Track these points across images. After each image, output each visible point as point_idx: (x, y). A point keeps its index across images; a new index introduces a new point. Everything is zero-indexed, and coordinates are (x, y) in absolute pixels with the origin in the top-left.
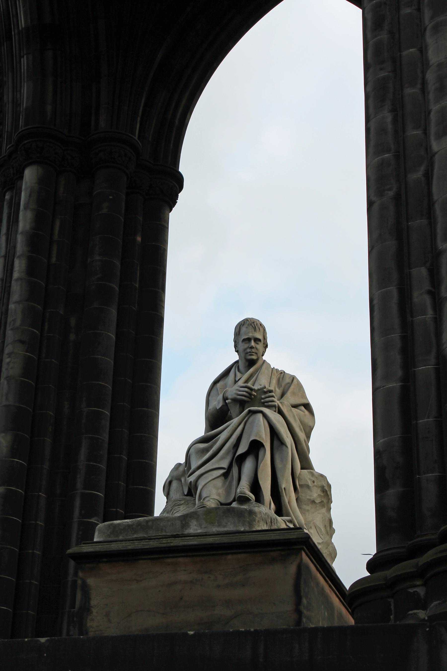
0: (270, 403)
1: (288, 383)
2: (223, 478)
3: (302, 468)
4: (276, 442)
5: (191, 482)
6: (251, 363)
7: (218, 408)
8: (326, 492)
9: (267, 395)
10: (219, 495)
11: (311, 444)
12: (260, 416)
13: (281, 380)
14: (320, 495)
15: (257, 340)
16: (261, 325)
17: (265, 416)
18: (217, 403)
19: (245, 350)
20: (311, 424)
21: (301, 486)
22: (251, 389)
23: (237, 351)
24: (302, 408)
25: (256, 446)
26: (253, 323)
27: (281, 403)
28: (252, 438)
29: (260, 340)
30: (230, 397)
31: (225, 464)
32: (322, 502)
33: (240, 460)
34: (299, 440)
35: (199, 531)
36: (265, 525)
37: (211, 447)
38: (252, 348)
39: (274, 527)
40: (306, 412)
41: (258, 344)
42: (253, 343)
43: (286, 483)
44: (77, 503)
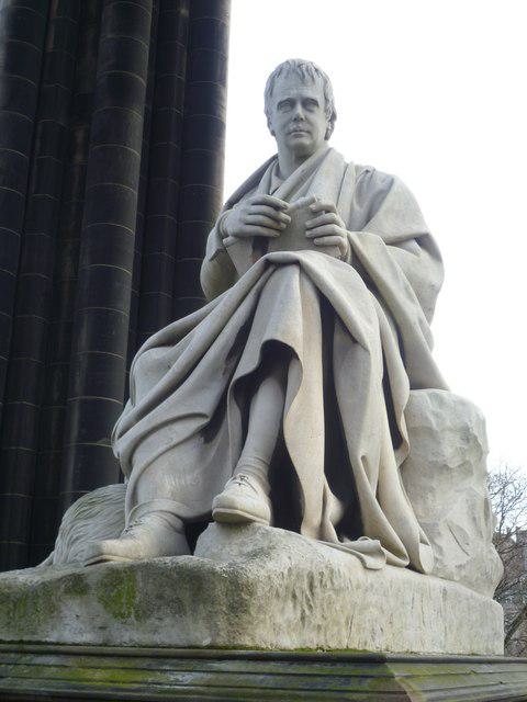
0: (326, 239)
3: (414, 386)
4: (338, 338)
9: (318, 219)
11: (436, 327)
12: (294, 275)
13: (365, 185)
15: (309, 103)
16: (316, 70)
19: (285, 126)
20: (434, 280)
22: (277, 208)
24: (414, 244)
25: (278, 358)
26: (299, 66)
27: (360, 236)
28: (267, 337)
29: (315, 102)
30: (230, 230)
31: (205, 403)
33: (245, 391)
34: (407, 321)
35: (87, 637)
37: (175, 358)
38: (297, 120)
40: (424, 255)
41: (311, 111)
42: (299, 110)
43: (371, 443)
44: (76, 417)
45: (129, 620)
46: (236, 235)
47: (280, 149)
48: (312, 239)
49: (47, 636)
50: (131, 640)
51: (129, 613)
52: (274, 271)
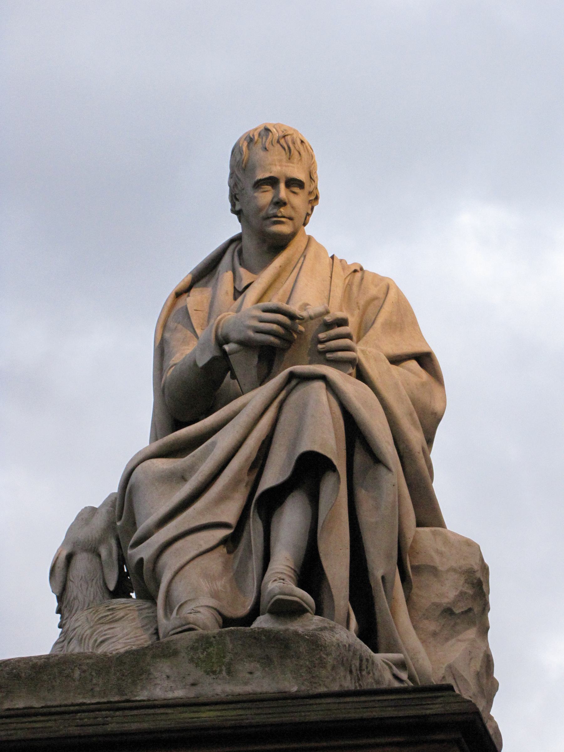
0: (340, 354)
1: (375, 298)
2: (223, 550)
4: (359, 458)
5: (141, 560)
6: (276, 245)
7: (201, 364)
8: (477, 585)
10: (215, 595)
13: (355, 289)
14: (466, 593)
15: (293, 183)
16: (302, 142)
17: (331, 387)
18: (190, 350)
20: (437, 407)
21: (417, 569)
23: (238, 213)
24: (413, 364)
25: (310, 469)
26: (284, 137)
29: (301, 184)
31: (230, 513)
32: (470, 610)
35: (179, 693)
36: (349, 678)
37: (192, 469)
38: (280, 203)
39: (368, 683)
40: (424, 375)
42: (283, 192)
45: (221, 676)
46: (240, 343)
47: (243, 230)
48: (324, 353)
49: (136, 696)
50: (223, 692)
51: (221, 671)
52: (297, 384)
